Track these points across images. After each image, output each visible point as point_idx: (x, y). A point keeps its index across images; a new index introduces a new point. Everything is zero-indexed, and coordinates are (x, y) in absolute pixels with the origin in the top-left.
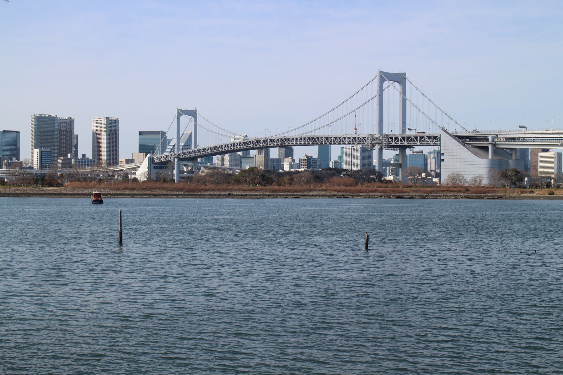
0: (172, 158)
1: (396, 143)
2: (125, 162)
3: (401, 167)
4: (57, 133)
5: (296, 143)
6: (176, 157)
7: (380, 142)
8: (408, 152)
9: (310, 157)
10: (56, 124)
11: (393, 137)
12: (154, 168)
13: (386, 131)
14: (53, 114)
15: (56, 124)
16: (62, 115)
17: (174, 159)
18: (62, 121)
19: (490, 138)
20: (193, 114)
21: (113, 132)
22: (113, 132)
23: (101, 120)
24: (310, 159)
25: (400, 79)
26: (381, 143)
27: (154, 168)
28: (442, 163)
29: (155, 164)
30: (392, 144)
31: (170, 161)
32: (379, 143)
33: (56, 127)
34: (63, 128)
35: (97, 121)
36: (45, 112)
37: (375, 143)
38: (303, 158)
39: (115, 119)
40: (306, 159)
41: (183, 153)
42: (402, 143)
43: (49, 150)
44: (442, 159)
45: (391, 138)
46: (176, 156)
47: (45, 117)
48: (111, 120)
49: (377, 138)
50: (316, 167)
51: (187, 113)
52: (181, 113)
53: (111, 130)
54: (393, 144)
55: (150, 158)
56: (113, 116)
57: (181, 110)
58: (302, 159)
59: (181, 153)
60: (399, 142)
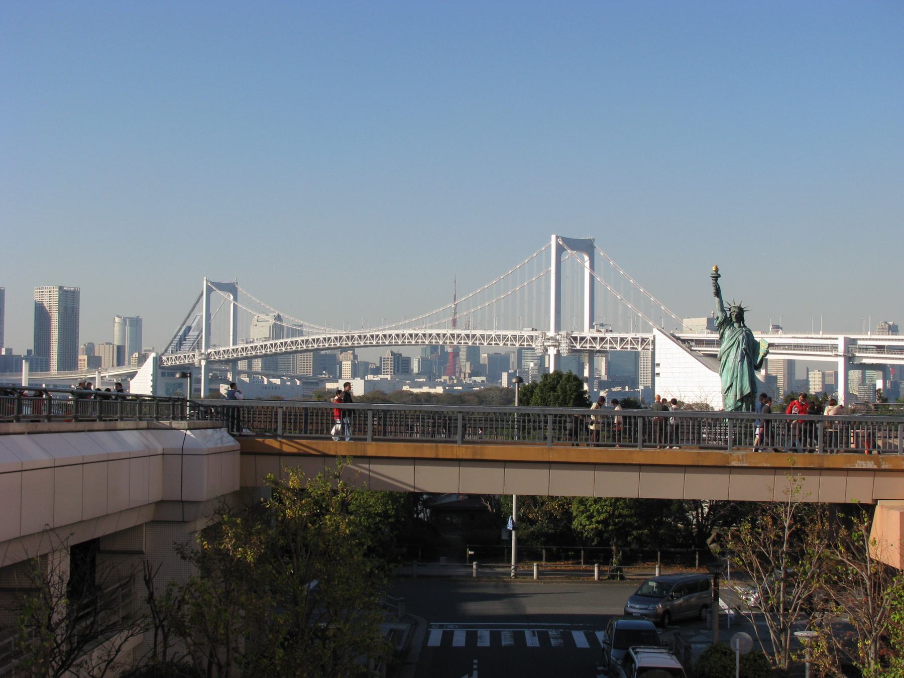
1: (582, 347)
2: (86, 360)
6: (204, 359)
7: (557, 344)
9: (397, 354)
17: (200, 362)
23: (50, 292)
24: (398, 358)
27: (163, 374)
28: (657, 379)
29: (164, 368)
31: (193, 364)
32: (555, 346)
35: (43, 292)
37: (549, 346)
38: (386, 357)
39: (72, 289)
40: (391, 358)
44: (656, 372)
45: (575, 338)
48: (66, 291)
50: (408, 372)
51: (223, 287)
53: (66, 308)
54: (578, 347)
56: (69, 286)
57: (212, 283)
58: (384, 358)
59: (213, 352)
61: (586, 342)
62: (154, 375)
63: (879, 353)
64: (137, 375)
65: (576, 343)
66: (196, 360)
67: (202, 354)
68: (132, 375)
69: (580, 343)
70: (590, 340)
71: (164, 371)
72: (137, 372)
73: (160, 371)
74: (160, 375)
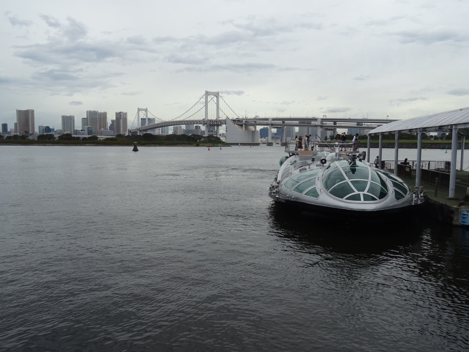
4: (98, 119)
8: (220, 127)
10: (98, 115)
13: (209, 118)
14: (96, 110)
15: (98, 115)
16: (101, 110)
18: (100, 114)
19: (244, 121)
20: (146, 110)
21: (124, 118)
22: (124, 118)
25: (217, 95)
33: (98, 116)
34: (102, 117)
36: (92, 110)
43: (91, 126)
45: (211, 121)
47: (92, 111)
52: (139, 110)
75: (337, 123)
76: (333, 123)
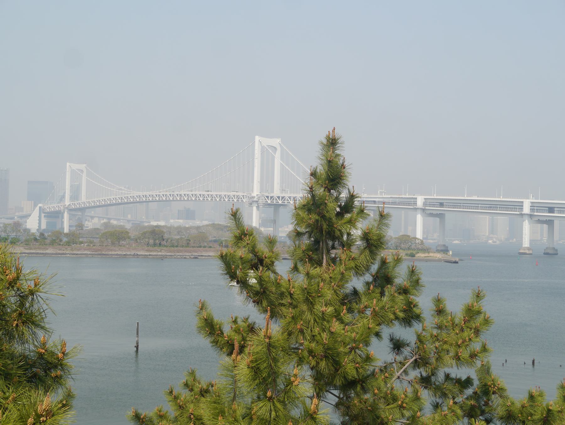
0: (62, 208)
1: (271, 202)
3: (275, 223)
5: (180, 199)
7: (257, 200)
8: (281, 209)
11: (268, 196)
12: (44, 217)
26: (258, 201)
27: (45, 216)
30: (268, 202)
37: (253, 201)
40: (184, 211)
41: (72, 204)
42: (276, 202)
45: (268, 197)
46: (66, 206)
49: (254, 197)
54: (269, 202)
55: (40, 207)
60: (275, 201)
61: (273, 200)
62: (40, 217)
63: (442, 207)
64: (31, 217)
65: (268, 200)
66: (62, 208)
67: (65, 205)
68: (30, 216)
69: (270, 200)
70: (276, 198)
71: (45, 215)
72: (31, 215)
73: (43, 215)
74: (43, 217)
75: (556, 209)
76: (547, 209)
